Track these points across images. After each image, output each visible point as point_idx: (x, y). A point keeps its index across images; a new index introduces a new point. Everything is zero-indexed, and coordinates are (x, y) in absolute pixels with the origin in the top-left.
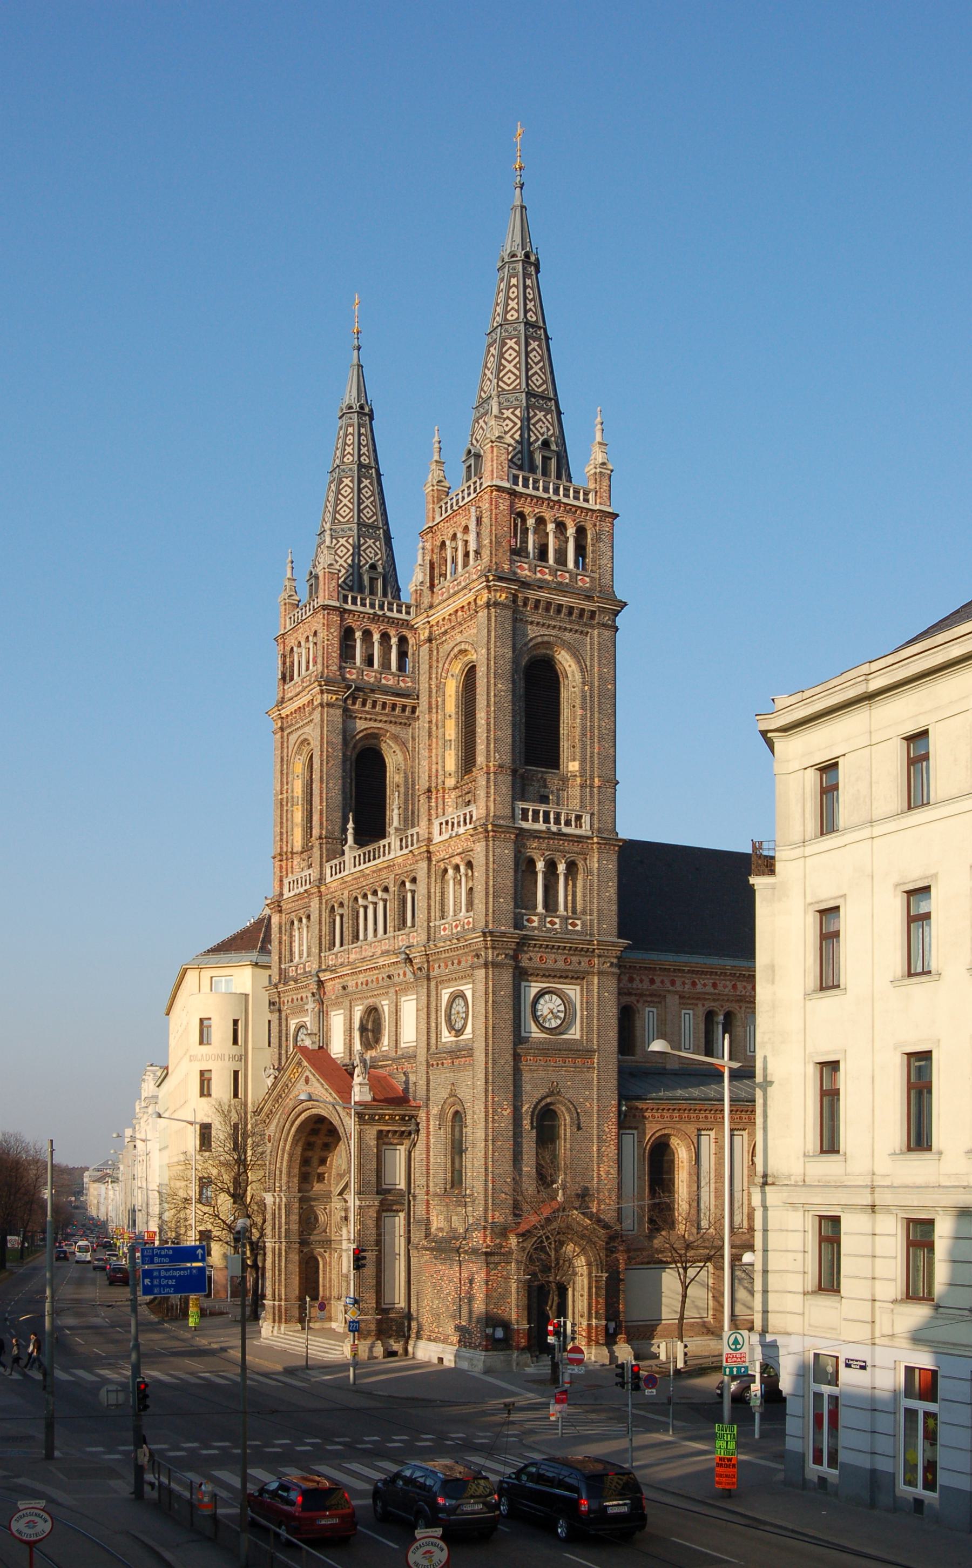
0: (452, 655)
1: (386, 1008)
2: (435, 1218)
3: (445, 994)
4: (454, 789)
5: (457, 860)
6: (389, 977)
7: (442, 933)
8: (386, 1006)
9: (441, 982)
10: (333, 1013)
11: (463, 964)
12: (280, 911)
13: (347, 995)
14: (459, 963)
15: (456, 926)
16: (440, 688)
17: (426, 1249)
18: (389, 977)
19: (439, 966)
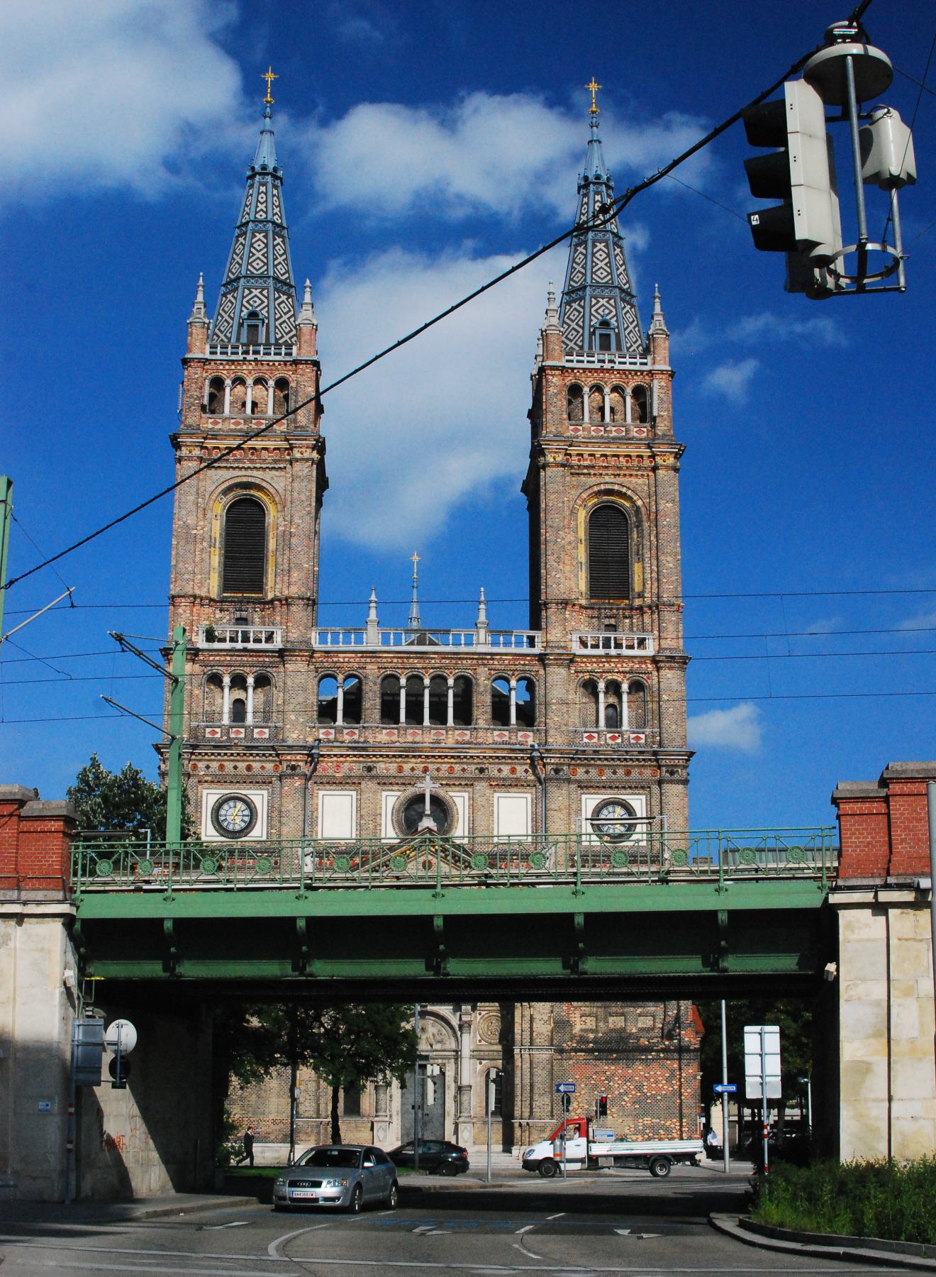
0: (596, 489)
1: (459, 801)
2: (578, 1019)
3: (590, 802)
4: (586, 608)
5: (618, 677)
6: (482, 770)
7: (586, 740)
8: (460, 800)
9: (585, 786)
10: (321, 793)
11: (635, 774)
12: (193, 661)
13: (373, 777)
14: (628, 773)
15: (613, 738)
16: (573, 512)
17: (581, 1051)
18: (482, 770)
19: (587, 772)
